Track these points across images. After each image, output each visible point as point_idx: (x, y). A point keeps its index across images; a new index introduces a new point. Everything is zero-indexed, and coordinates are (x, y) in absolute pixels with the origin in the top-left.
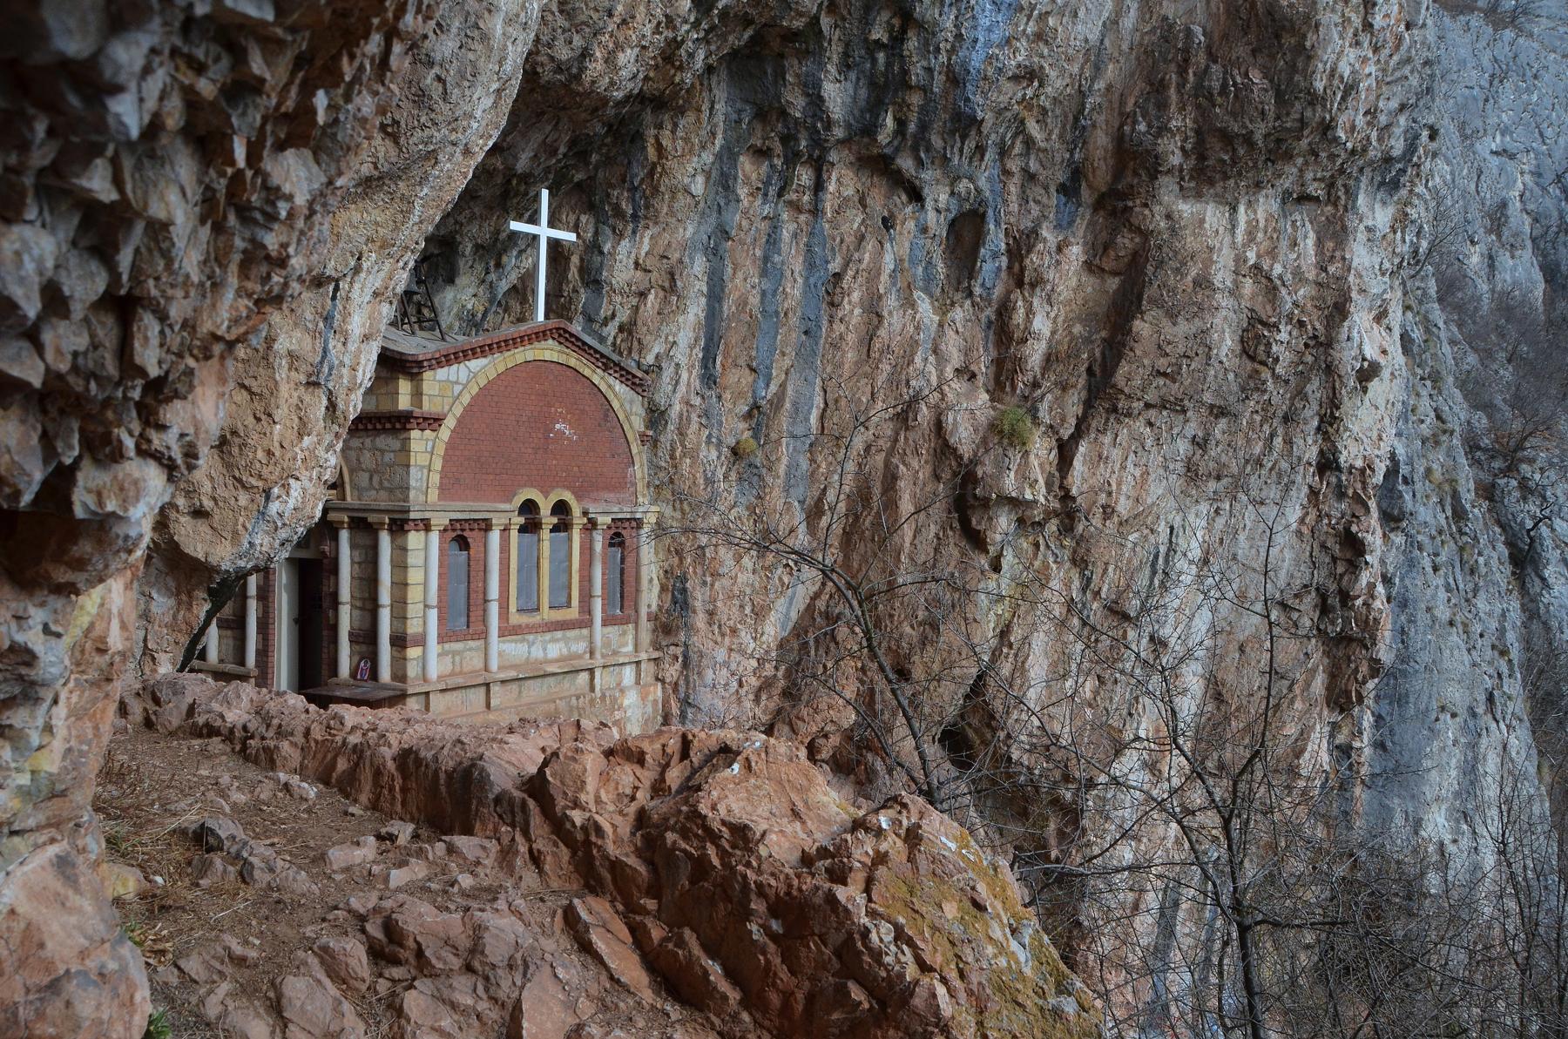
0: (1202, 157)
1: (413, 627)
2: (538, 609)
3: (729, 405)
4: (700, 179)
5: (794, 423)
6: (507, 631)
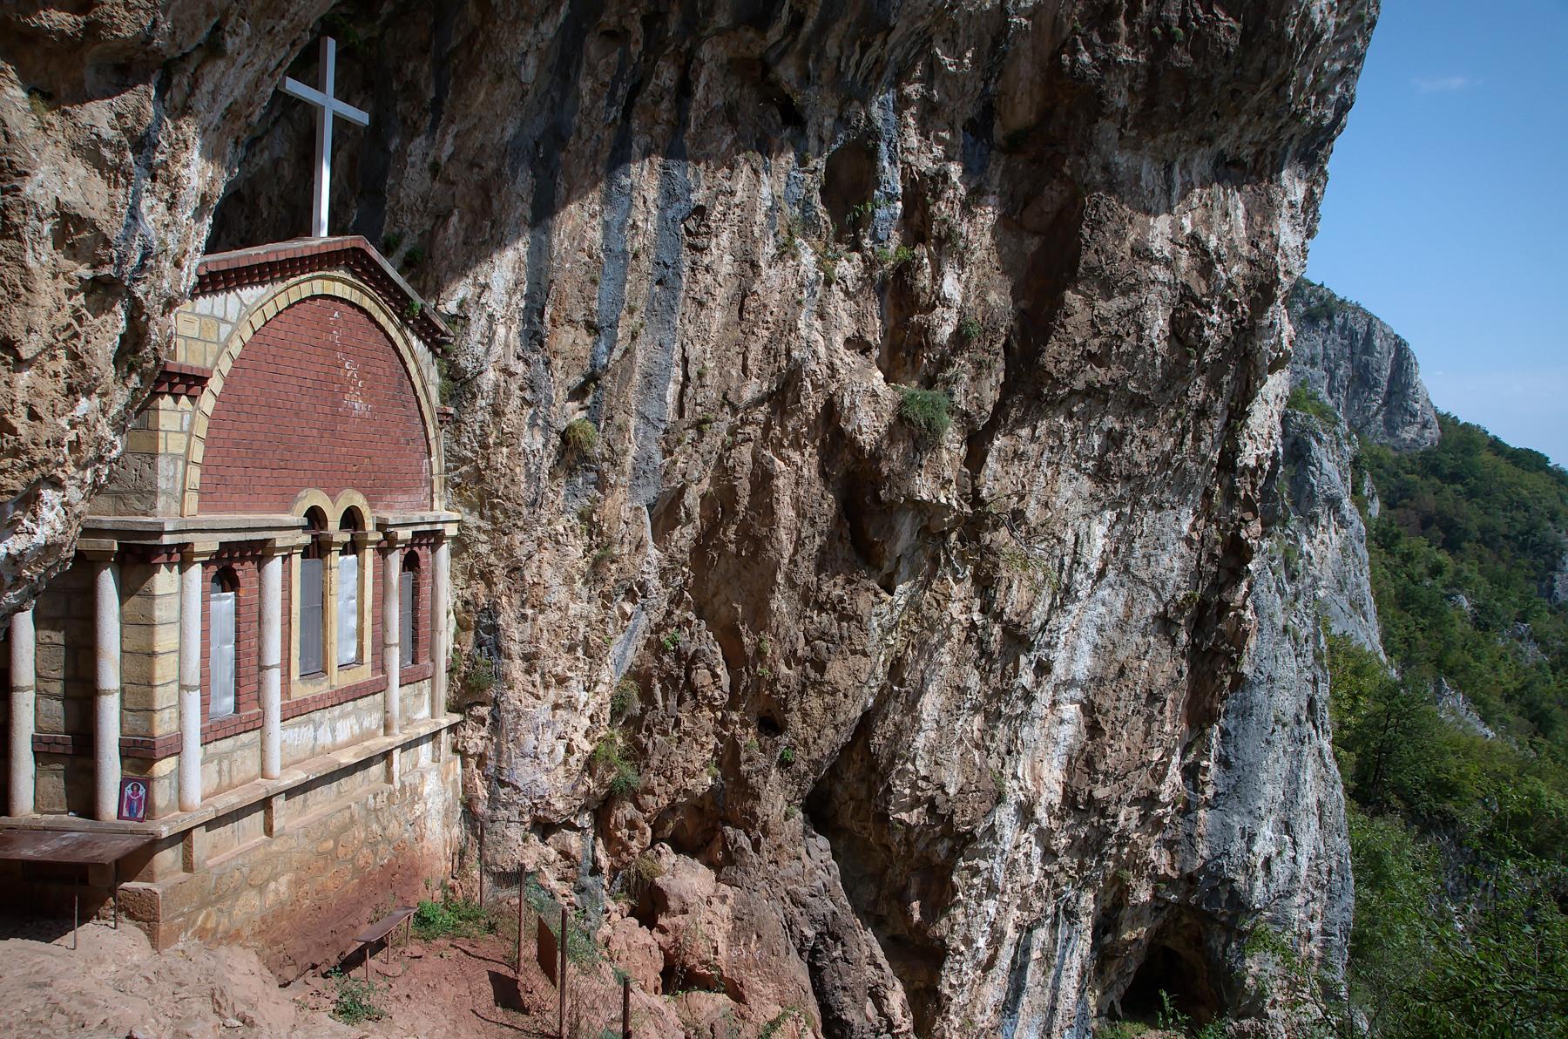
0: (1151, 103)
1: (163, 725)
2: (325, 672)
3: (559, 375)
4: (531, 61)
5: (645, 401)
6: (294, 712)
